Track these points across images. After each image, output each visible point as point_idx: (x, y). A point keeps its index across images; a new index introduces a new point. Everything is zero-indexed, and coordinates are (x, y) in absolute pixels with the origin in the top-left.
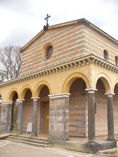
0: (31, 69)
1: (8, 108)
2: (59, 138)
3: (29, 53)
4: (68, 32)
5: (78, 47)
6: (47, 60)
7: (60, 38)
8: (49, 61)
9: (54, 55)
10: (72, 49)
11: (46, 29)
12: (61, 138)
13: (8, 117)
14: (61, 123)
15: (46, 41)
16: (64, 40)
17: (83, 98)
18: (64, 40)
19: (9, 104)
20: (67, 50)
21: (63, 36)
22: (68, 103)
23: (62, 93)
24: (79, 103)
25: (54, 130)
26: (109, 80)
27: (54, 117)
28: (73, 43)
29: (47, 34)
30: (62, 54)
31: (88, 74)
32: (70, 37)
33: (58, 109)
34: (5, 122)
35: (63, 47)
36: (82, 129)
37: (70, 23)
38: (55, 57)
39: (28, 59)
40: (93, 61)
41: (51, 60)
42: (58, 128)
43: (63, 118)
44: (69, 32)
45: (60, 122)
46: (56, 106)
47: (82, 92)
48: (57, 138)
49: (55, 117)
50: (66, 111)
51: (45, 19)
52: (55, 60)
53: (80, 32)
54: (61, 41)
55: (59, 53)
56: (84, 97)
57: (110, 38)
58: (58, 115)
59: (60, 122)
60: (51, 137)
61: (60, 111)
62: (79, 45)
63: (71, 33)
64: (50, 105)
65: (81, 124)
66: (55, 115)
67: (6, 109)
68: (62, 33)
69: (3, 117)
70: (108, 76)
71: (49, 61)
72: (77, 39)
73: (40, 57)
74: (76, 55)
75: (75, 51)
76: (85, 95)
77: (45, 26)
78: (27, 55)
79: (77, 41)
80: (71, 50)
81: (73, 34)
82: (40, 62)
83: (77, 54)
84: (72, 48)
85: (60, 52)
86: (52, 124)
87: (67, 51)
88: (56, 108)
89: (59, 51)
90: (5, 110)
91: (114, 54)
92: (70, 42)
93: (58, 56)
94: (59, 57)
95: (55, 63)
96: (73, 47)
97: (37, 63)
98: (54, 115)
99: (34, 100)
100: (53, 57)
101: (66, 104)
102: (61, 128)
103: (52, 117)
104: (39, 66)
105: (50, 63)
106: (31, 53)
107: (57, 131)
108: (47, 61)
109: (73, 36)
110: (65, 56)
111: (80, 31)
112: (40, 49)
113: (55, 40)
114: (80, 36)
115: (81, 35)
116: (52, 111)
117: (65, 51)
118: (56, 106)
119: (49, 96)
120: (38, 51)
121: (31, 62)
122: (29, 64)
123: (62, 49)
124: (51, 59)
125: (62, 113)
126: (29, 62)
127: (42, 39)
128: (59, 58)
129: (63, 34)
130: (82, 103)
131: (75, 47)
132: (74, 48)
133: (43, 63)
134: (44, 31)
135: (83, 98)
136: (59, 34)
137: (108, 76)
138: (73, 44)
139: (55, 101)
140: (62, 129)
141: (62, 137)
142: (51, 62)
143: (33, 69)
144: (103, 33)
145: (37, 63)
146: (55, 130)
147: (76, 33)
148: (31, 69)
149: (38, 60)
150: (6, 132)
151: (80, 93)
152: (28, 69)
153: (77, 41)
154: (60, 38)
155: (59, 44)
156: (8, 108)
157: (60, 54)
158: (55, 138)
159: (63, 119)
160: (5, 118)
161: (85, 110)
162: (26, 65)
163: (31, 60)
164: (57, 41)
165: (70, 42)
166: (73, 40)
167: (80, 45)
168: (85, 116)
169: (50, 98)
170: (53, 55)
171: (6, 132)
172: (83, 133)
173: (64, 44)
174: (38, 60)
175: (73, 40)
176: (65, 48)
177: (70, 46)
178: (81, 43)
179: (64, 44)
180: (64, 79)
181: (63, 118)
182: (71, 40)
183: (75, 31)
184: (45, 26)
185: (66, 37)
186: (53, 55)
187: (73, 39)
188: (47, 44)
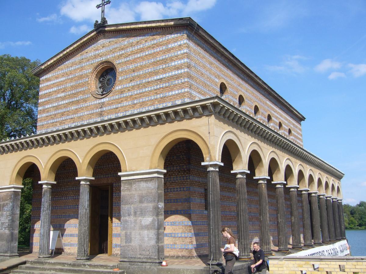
0: (63, 114)
1: (13, 202)
2: (144, 260)
3: (57, 78)
4: (152, 43)
5: (175, 75)
6: (101, 98)
7: (133, 53)
8: (107, 99)
9: (120, 87)
10: (161, 79)
11: (101, 29)
12: (149, 261)
13: (13, 221)
14: (148, 229)
17: (185, 178)
19: (14, 191)
20: (150, 80)
21: (142, 50)
22: (162, 190)
23: (151, 168)
24: (177, 188)
25: (133, 244)
26: (240, 145)
27: (132, 217)
28: (164, 66)
30: (138, 86)
31: (208, 135)
32: (158, 53)
33: (141, 202)
34: (5, 233)
35: (141, 73)
36: (183, 242)
37: (158, 24)
38: (122, 92)
39: (55, 91)
40: (218, 110)
41: (112, 98)
42: (142, 239)
43: (153, 220)
44: (155, 42)
45: (147, 227)
46: (136, 195)
47: (183, 166)
48: (140, 260)
49: (135, 218)
50: (160, 206)
51: (98, 7)
52: (121, 98)
53: (180, 45)
54: (135, 59)
55: (130, 85)
56: (186, 176)
57: (232, 58)
58: (143, 213)
59: (147, 227)
60: (125, 260)
61: (145, 205)
62: (177, 72)
63: (158, 45)
64: (122, 193)
65: (181, 231)
66: (135, 213)
67: (7, 204)
68: (138, 42)
70: (238, 138)
71: (107, 99)
72: (171, 59)
73: (84, 91)
74: (169, 92)
75: (167, 84)
76: (190, 172)
77: (97, 22)
78: (52, 82)
79: (173, 64)
80: (158, 80)
81: (164, 48)
82: (85, 100)
83: (172, 90)
84: (161, 77)
85: (133, 84)
86: (128, 232)
87: (149, 82)
88: (137, 199)
89: (131, 81)
90: (4, 206)
91: (237, 91)
92: (155, 63)
93: (129, 90)
94: (130, 94)
95: (122, 105)
96: (164, 76)
97: (78, 102)
98: (132, 213)
99: (82, 183)
100: (116, 91)
101: (159, 192)
102: (150, 239)
103: (127, 218)
104: (82, 109)
105: (110, 105)
106: (62, 79)
107: (140, 246)
108: (102, 100)
109: (164, 52)
110: (144, 92)
111: (179, 43)
112: (85, 72)
113: (121, 55)
114: (179, 53)
116: (127, 206)
117: (144, 81)
118: (136, 195)
119: (119, 174)
120: (81, 77)
122: (56, 104)
123: (139, 77)
124: (113, 96)
125: (151, 209)
126: (57, 99)
127: (90, 51)
128: (132, 95)
129: (141, 46)
130: (183, 188)
131: (167, 75)
132: (164, 78)
133: (93, 103)
134: (95, 33)
135: (185, 178)
136: (132, 45)
137: (238, 138)
138: (163, 69)
139: (134, 186)
140: (153, 242)
141: (152, 258)
142: (112, 103)
143: (68, 115)
144: (220, 48)
145: (78, 102)
146: (135, 243)
147: (170, 46)
148: (63, 114)
149: (81, 97)
150: (6, 254)
151: (178, 168)
152: (55, 115)
153: (173, 64)
154: (133, 53)
155: (132, 67)
156: (12, 201)
157: (133, 86)
158: (136, 260)
159: (152, 221)
161: (190, 202)
162: (50, 106)
163: (63, 95)
164: (126, 60)
165: (155, 63)
166: (164, 61)
167: (180, 72)
168: (190, 214)
169: (122, 179)
170: (117, 88)
171: (6, 254)
172: (187, 249)
173: (142, 67)
174: (81, 97)
175: (163, 59)
176: (145, 76)
177: (156, 73)
178: (182, 68)
179: (142, 67)
180: (154, 140)
181: (154, 219)
182: (158, 59)
183: (168, 42)
184: (97, 22)
185: (147, 53)
186: (118, 88)
187: (164, 57)
188: (102, 63)
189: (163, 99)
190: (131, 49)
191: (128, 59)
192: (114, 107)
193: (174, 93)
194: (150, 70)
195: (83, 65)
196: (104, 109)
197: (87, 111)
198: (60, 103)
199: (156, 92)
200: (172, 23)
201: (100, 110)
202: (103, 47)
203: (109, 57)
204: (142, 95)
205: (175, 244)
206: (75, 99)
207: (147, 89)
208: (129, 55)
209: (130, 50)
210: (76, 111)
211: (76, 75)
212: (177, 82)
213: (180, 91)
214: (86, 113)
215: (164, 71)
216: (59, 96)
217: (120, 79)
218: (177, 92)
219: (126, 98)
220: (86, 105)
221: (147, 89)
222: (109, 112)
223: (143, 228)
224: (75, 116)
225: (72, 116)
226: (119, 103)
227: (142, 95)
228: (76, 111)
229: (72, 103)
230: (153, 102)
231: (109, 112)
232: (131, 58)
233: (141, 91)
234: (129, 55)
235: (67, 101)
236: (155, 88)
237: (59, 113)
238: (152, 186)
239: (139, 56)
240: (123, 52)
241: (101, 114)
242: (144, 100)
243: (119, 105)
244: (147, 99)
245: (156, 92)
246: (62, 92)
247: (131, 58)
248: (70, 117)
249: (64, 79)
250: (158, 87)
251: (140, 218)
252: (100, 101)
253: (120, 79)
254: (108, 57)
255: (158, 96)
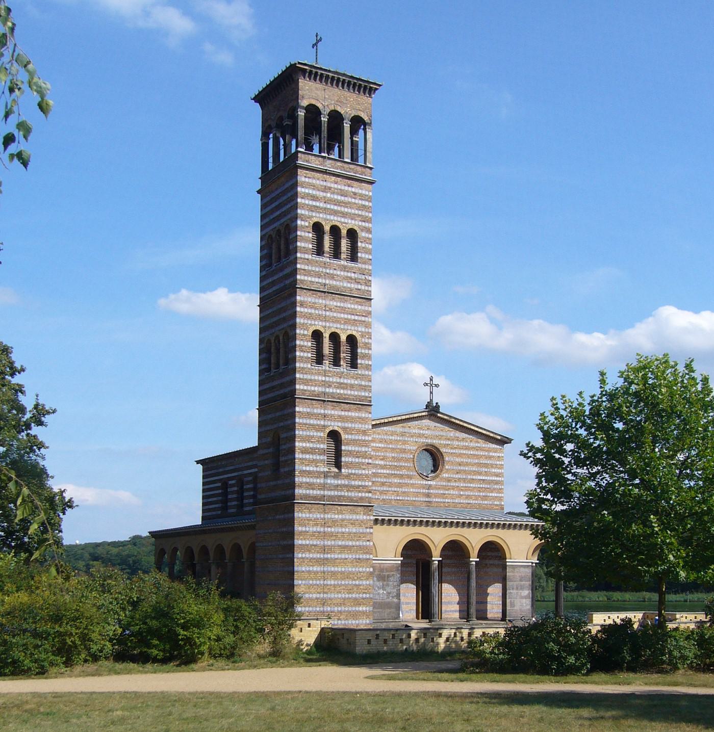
0: (383, 484)
4: (477, 445)
7: (458, 447)
8: (434, 483)
10: (484, 480)
15: (426, 437)
16: (468, 456)
18: (468, 456)
20: (474, 477)
21: (467, 448)
25: (515, 608)
28: (486, 470)
29: (426, 422)
30: (464, 480)
32: (481, 456)
33: (521, 580)
38: (449, 480)
41: (439, 483)
44: (479, 445)
45: (525, 597)
58: (522, 588)
59: (525, 597)
62: (496, 479)
63: (482, 449)
67: (393, 575)
69: (381, 591)
72: (492, 466)
81: (486, 453)
82: (410, 477)
83: (492, 492)
84: (484, 478)
88: (519, 579)
89: (457, 473)
90: (388, 576)
92: (479, 465)
93: (455, 481)
96: (486, 478)
97: (401, 476)
104: (407, 485)
108: (429, 483)
111: (498, 455)
112: (408, 447)
113: (448, 445)
114: (498, 463)
115: (500, 463)
117: (469, 477)
121: (383, 467)
123: (465, 471)
127: (414, 426)
128: (458, 487)
129: (467, 444)
131: (489, 478)
136: (457, 439)
138: (485, 472)
139: (516, 570)
142: (439, 488)
143: (389, 486)
145: (401, 476)
146: (517, 608)
148: (383, 484)
153: (493, 470)
154: (458, 447)
155: (458, 460)
156: (400, 572)
160: (389, 593)
163: (382, 463)
165: (479, 465)
166: (486, 465)
167: (498, 479)
170: (444, 475)
173: (467, 464)
174: (404, 472)
176: (470, 472)
177: (480, 473)
179: (467, 464)
182: (481, 462)
183: (489, 450)
189: (485, 498)
190: (457, 443)
191: (454, 451)
192: (442, 492)
193: (493, 495)
194: (474, 469)
195: (406, 439)
196: (432, 491)
197: (413, 488)
198: (379, 471)
199: (480, 490)
200: (499, 438)
201: (427, 491)
202: (428, 429)
203: (436, 442)
204: (467, 489)
205: (493, 609)
206: (398, 472)
207: (472, 485)
208: (456, 448)
209: (456, 443)
210: (400, 485)
211: (399, 447)
212: (496, 487)
213: (498, 495)
214: (411, 490)
215: (486, 474)
216: (377, 463)
217: (447, 467)
218: (496, 495)
219: (453, 488)
220: (411, 482)
221: (472, 485)
222: (436, 496)
223: (522, 597)
224: (398, 489)
225: (396, 489)
226: (446, 490)
227: (467, 489)
228: (400, 485)
229: (395, 476)
230: (477, 498)
231: (436, 496)
232: (457, 451)
233: (467, 485)
234: (456, 448)
235: (388, 472)
236: (479, 486)
237: (377, 482)
238: (529, 572)
239: (464, 452)
240: (449, 443)
241: (428, 495)
242: (469, 494)
243: (447, 492)
244: (472, 494)
245: (480, 490)
246: (382, 460)
247: (457, 451)
248: (393, 489)
249: (383, 446)
250: (481, 486)
251: (521, 591)
252: (427, 483)
253: (447, 467)
254: (434, 441)
255: (481, 494)
